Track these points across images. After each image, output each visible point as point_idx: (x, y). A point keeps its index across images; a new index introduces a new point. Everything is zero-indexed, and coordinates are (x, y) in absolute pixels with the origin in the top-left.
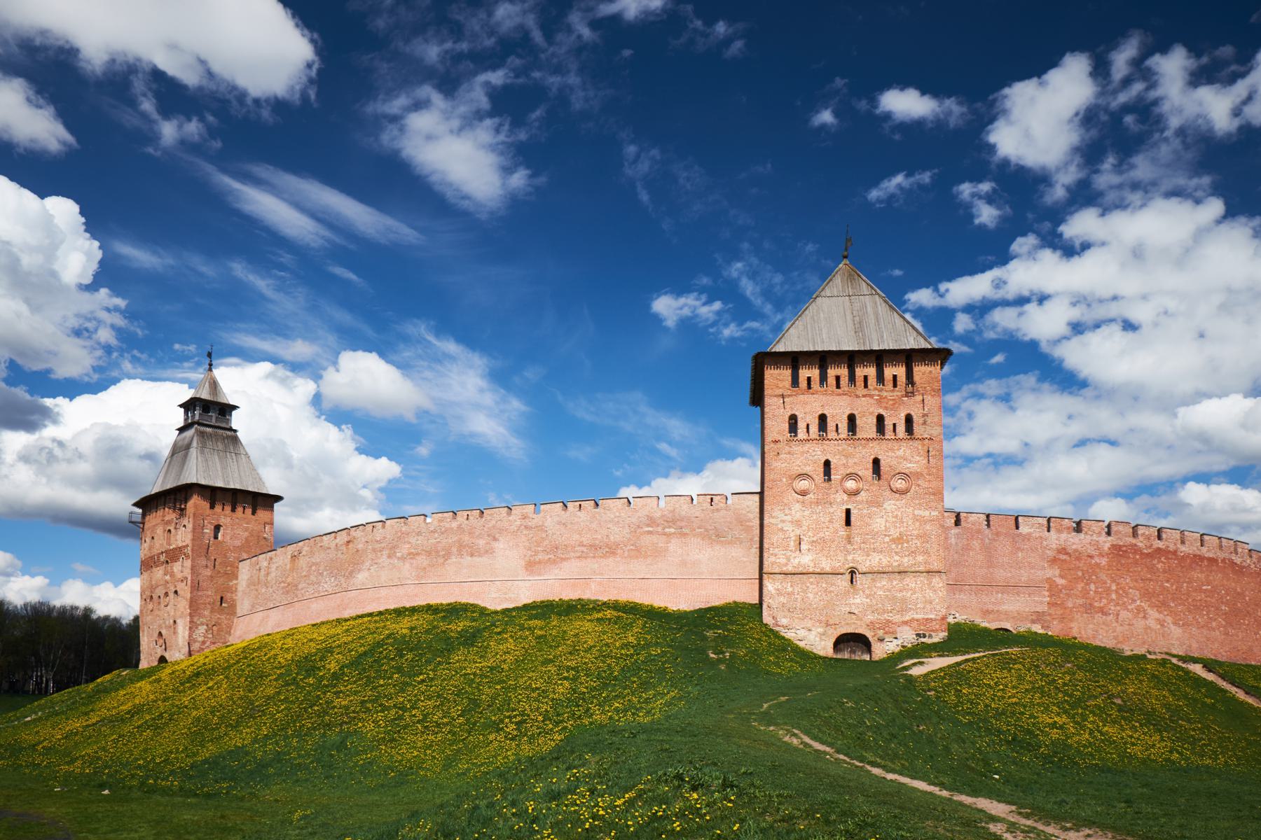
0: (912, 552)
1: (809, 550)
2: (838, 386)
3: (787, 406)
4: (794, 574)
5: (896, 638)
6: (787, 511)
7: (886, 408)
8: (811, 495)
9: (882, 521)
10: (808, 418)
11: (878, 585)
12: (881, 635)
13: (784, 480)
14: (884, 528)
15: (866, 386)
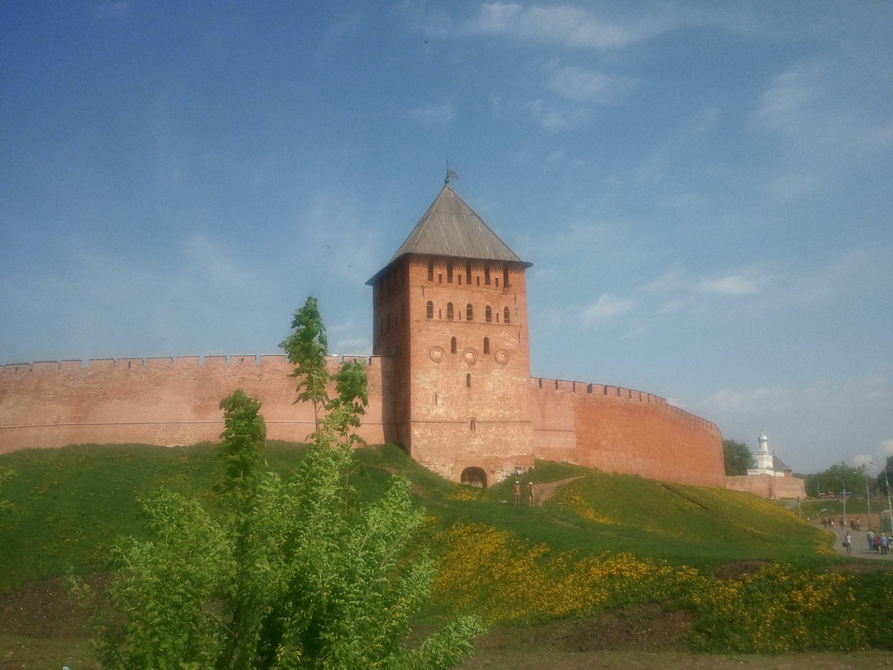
0: (511, 407)
1: (443, 403)
2: (460, 283)
5: (503, 471)
6: (427, 374)
7: (492, 302)
10: (440, 306)
11: (490, 431)
12: (493, 468)
13: (425, 350)
14: (492, 389)
15: (478, 285)
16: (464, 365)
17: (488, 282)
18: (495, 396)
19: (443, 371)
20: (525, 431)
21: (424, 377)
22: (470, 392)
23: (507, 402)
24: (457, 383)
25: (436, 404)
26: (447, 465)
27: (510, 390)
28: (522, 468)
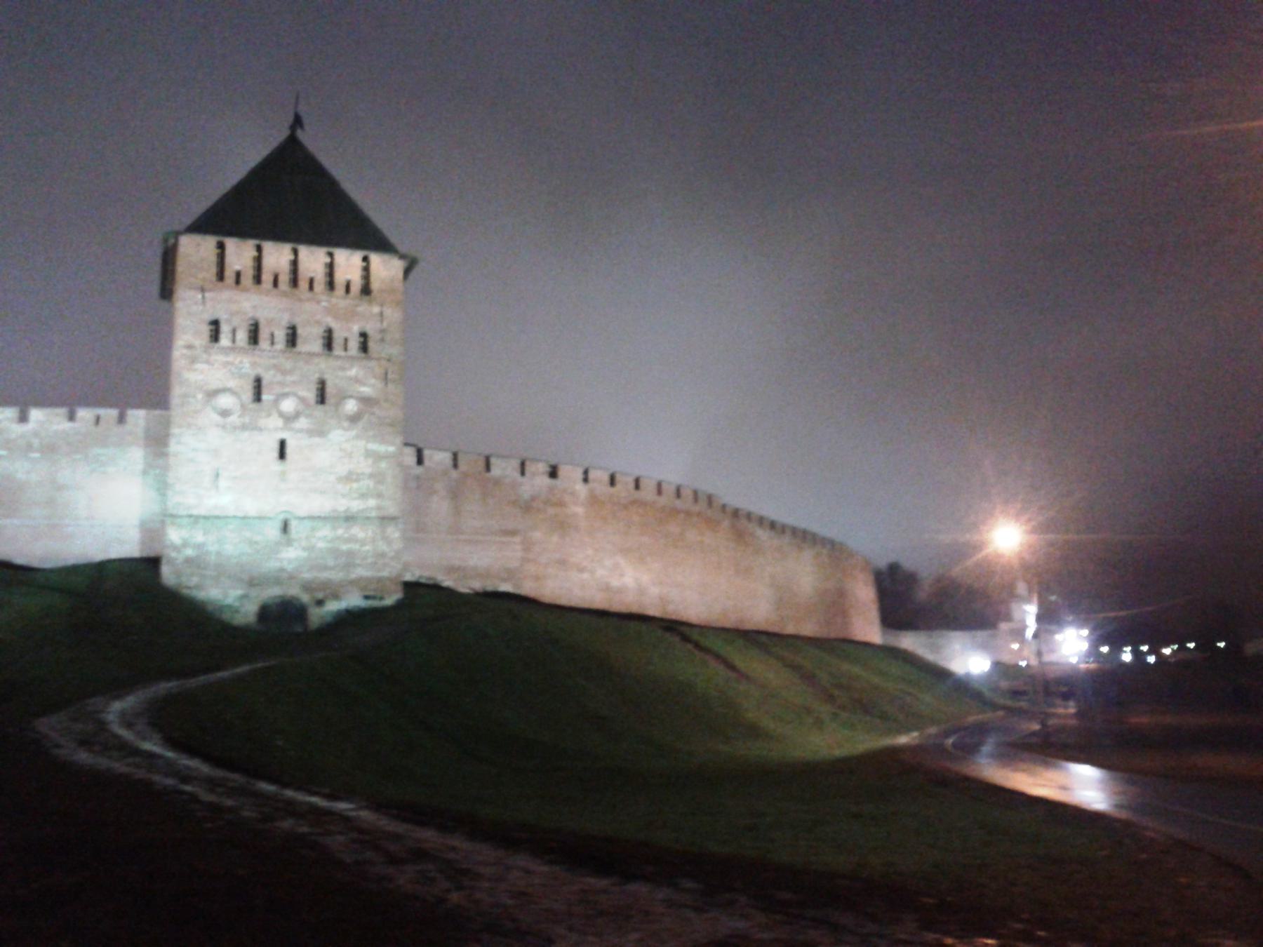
3: (209, 304)
7: (336, 317)
16: (275, 422)
25: (217, 487)
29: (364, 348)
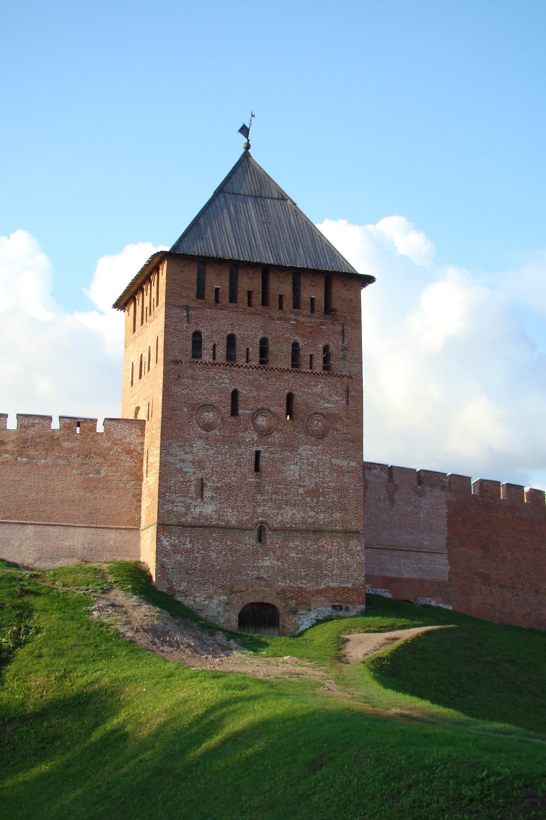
1: (213, 497)
2: (250, 304)
4: (195, 527)
6: (188, 449)
7: (303, 336)
8: (216, 431)
9: (296, 468)
13: (186, 410)
14: (298, 478)
15: (281, 308)
16: (251, 436)
17: (297, 304)
18: (302, 489)
19: (216, 444)
20: (350, 546)
21: (183, 452)
22: (259, 481)
23: (321, 499)
24: (238, 465)
25: (202, 497)
26: (215, 597)
27: (328, 480)
28: (344, 606)
29: (327, 367)
